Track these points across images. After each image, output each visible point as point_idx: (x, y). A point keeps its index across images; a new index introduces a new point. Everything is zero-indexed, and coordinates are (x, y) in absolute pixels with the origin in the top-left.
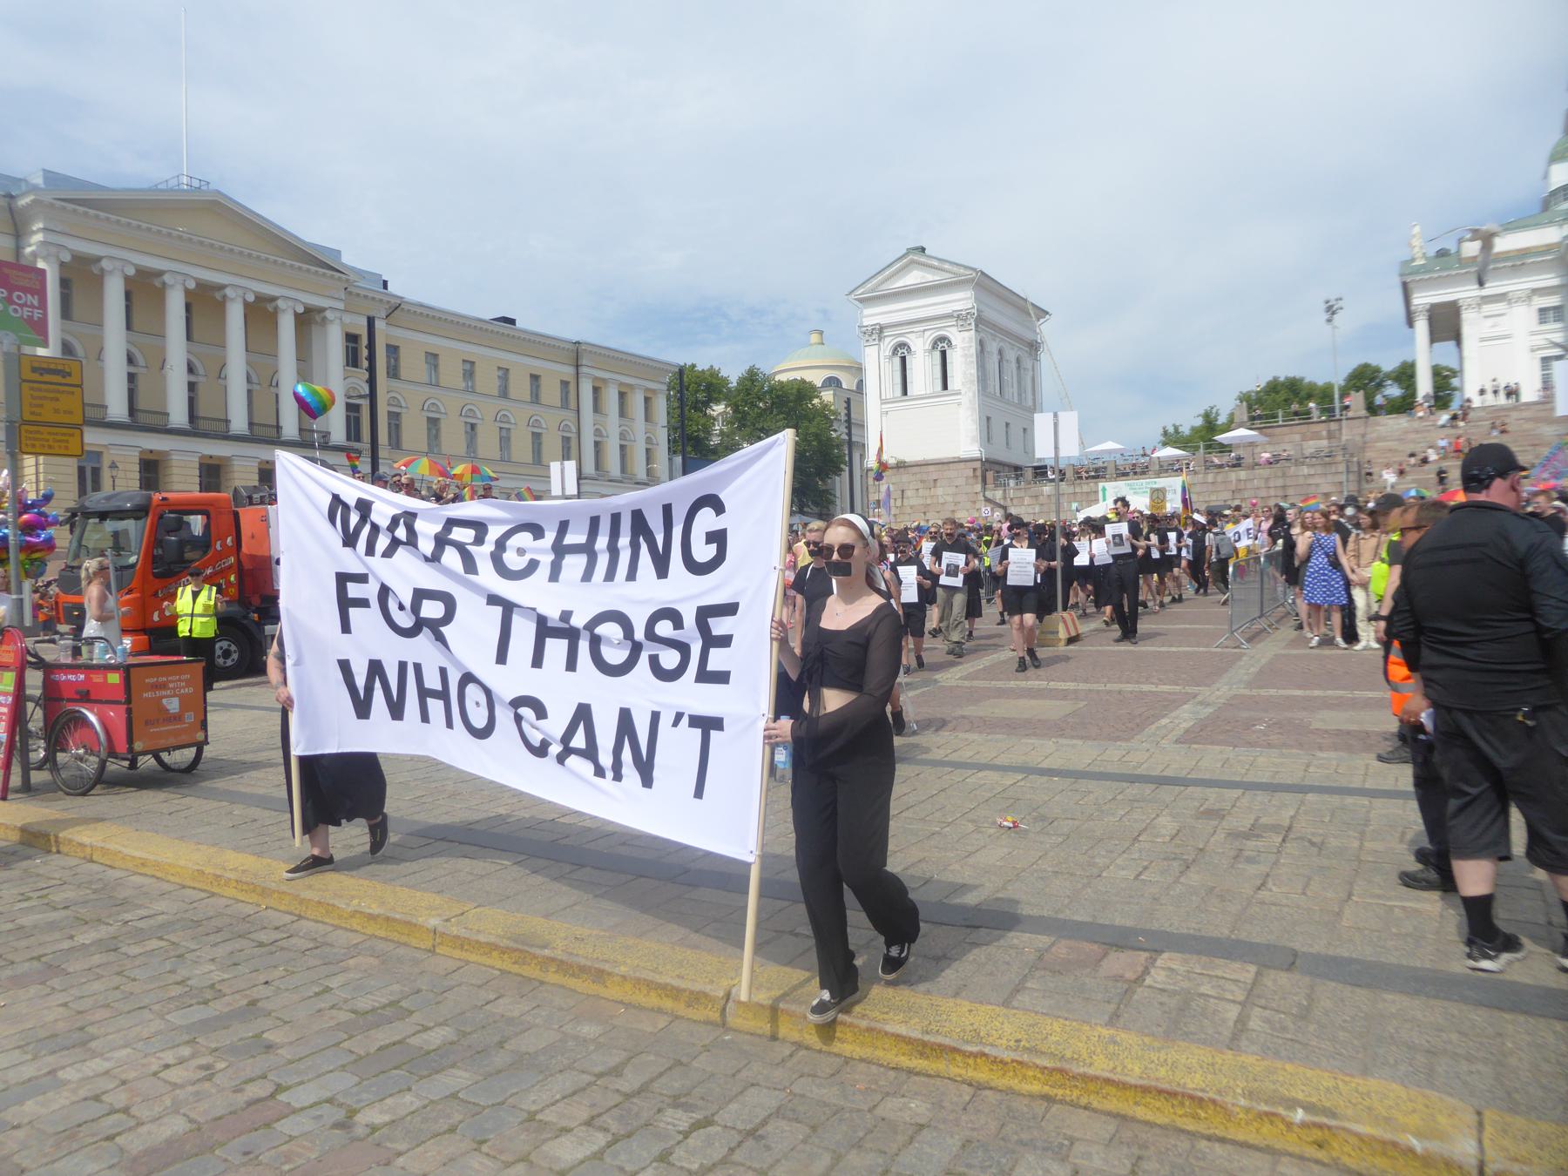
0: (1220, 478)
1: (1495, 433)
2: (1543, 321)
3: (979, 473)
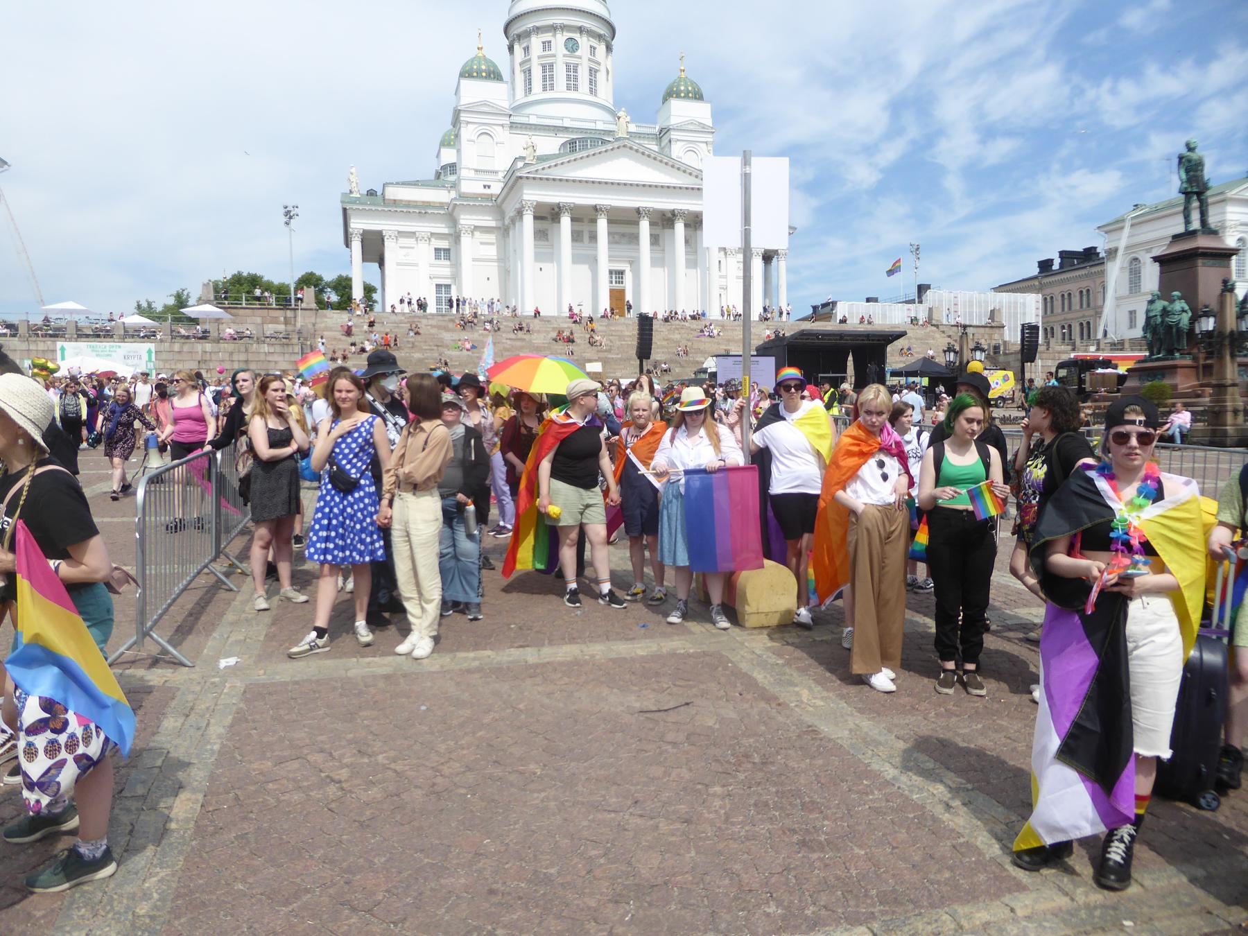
0: (186, 348)
1: (412, 334)
2: (437, 257)
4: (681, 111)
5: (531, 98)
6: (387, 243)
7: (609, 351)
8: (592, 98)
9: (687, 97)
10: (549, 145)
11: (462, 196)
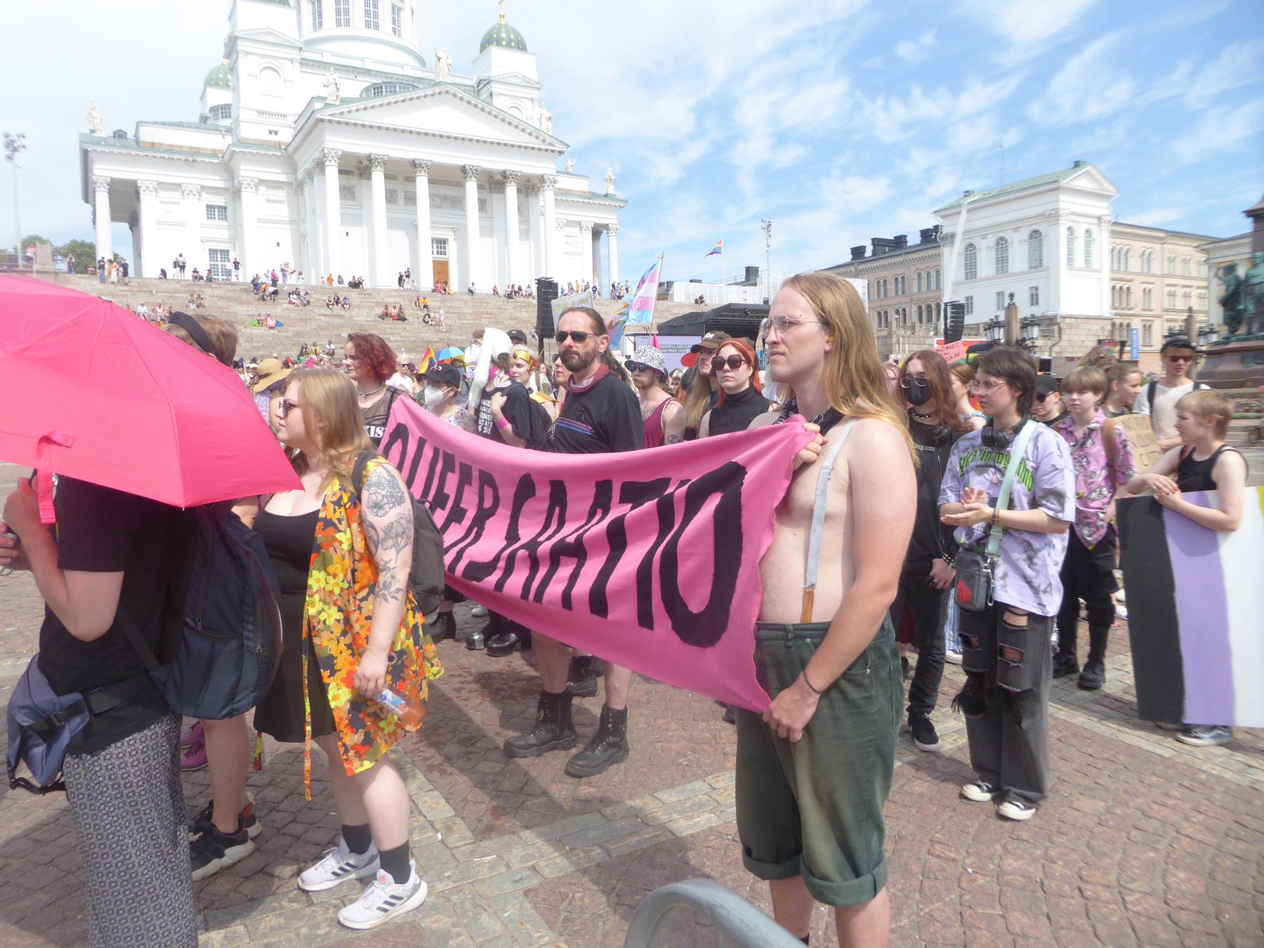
4: (501, 61)
5: (321, 33)
6: (144, 196)
7: (449, 331)
8: (395, 39)
9: (508, 46)
10: (352, 87)
11: (240, 142)
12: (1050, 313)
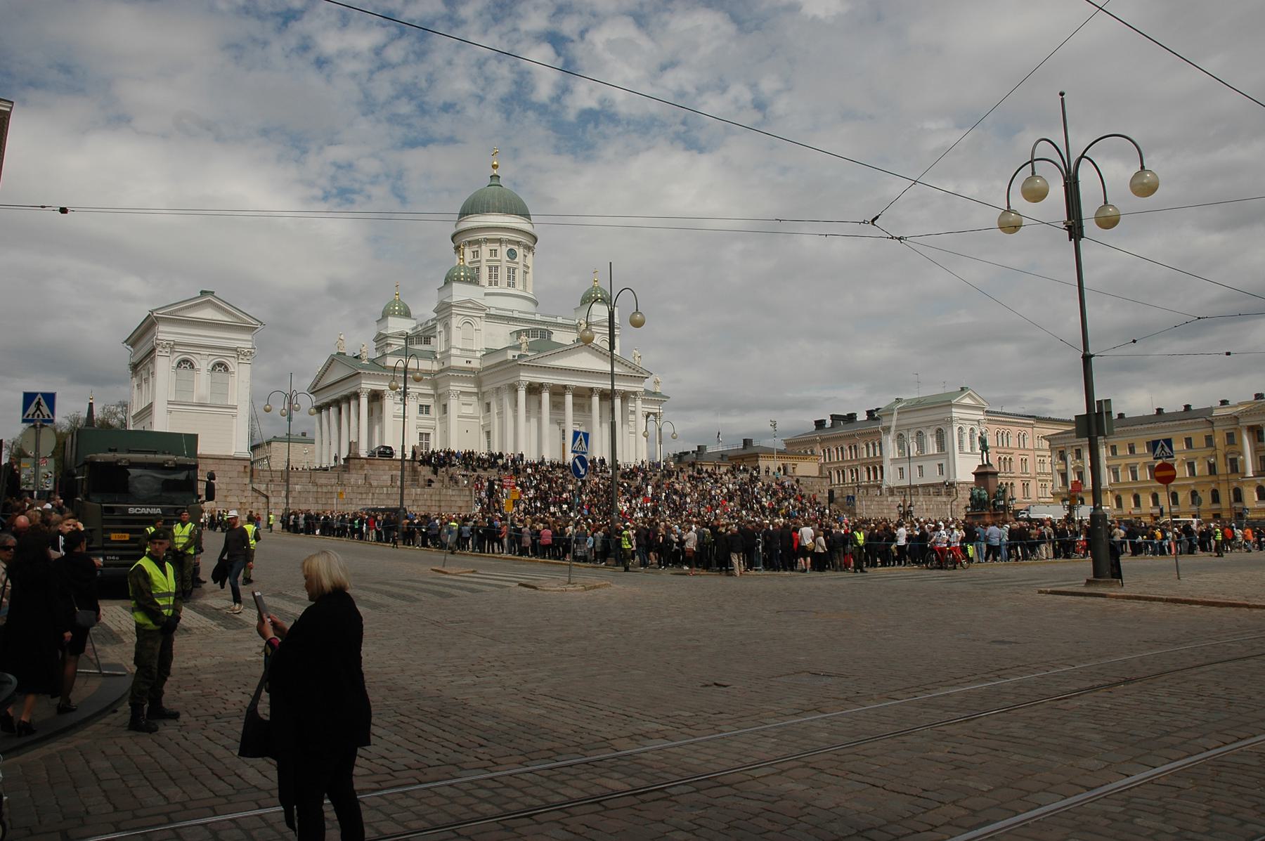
2: (421, 412)
3: (248, 470)
12: (951, 480)
